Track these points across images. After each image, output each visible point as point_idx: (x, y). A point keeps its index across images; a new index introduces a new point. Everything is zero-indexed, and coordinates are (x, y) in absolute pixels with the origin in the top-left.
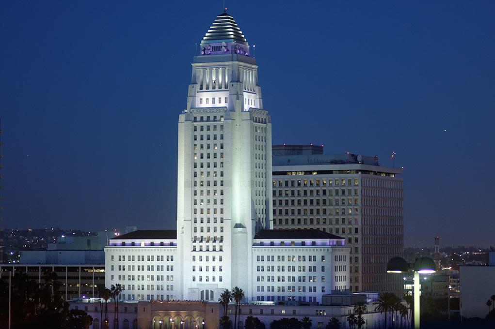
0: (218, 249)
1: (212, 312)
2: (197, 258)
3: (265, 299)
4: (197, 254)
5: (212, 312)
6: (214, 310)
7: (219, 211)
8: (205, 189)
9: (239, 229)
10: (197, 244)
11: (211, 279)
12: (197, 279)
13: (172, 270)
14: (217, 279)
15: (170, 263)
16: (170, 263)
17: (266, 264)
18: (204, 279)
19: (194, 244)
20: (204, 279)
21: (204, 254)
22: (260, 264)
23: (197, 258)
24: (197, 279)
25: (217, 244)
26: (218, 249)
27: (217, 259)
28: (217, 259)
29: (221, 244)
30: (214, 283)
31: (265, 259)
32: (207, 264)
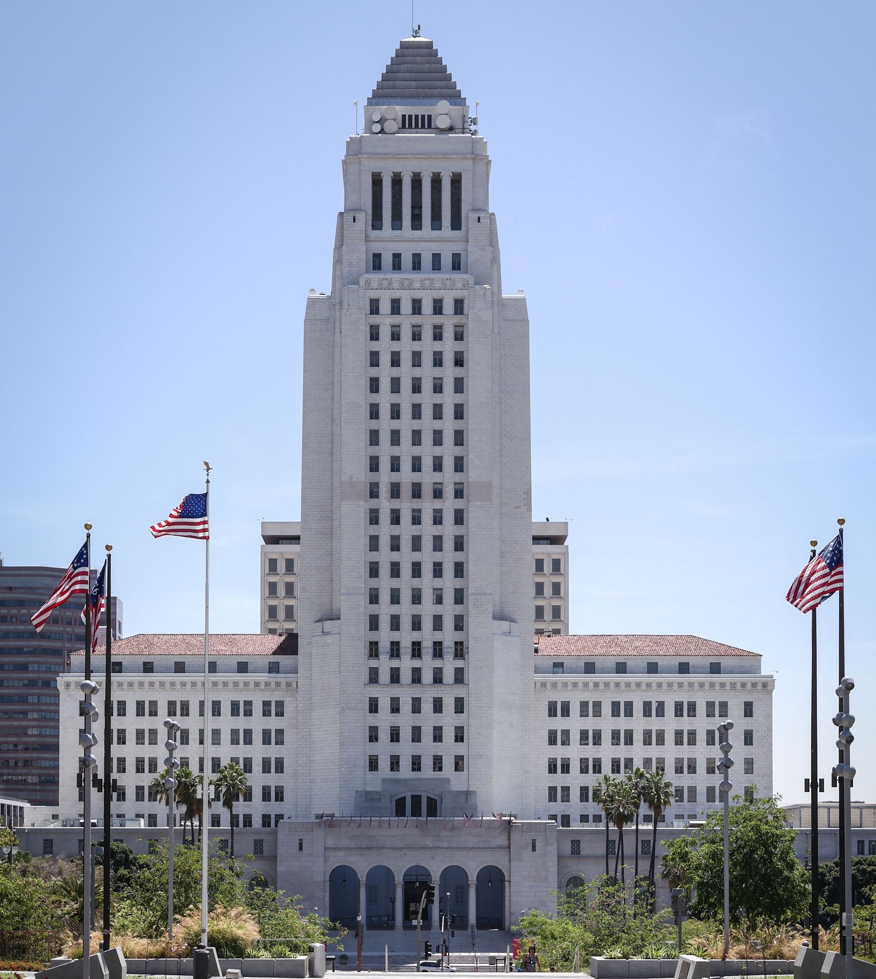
0: (449, 676)
1: (534, 849)
2: (384, 705)
3: (301, 842)
4: (384, 694)
5: (534, 849)
6: (538, 844)
7: (448, 570)
9: (505, 625)
10: (385, 664)
11: (427, 763)
12: (384, 764)
13: (280, 742)
14: (448, 763)
15: (273, 723)
16: (273, 723)
17: (575, 724)
18: (406, 764)
19: (373, 663)
20: (406, 764)
21: (406, 694)
22: (559, 723)
23: (384, 705)
24: (384, 764)
25: (449, 665)
26: (449, 676)
27: (449, 705)
28: (449, 705)
29: (460, 664)
30: (437, 774)
31: (575, 709)
32: (416, 719)
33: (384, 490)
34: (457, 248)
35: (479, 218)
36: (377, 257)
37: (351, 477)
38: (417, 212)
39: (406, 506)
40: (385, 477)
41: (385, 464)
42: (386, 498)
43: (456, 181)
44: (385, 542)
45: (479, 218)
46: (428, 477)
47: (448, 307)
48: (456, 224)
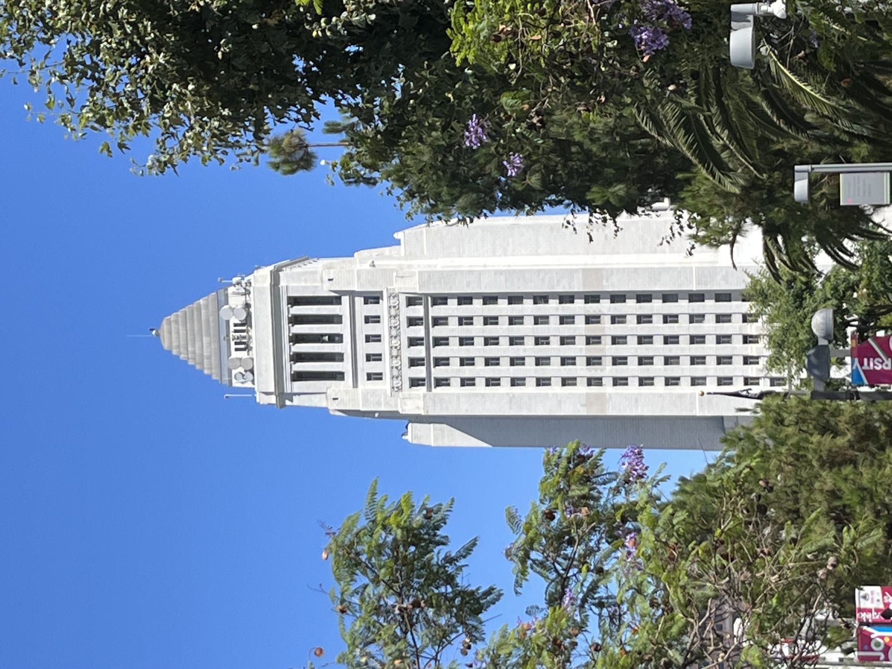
8: (608, 350)
33: (594, 371)
34: (359, 301)
35: (330, 280)
36: (370, 377)
37: (582, 405)
38: (326, 338)
39: (608, 350)
40: (581, 370)
41: (568, 371)
42: (602, 370)
43: (295, 301)
44: (645, 371)
45: (330, 280)
46: (579, 328)
47: (418, 311)
48: (335, 300)
